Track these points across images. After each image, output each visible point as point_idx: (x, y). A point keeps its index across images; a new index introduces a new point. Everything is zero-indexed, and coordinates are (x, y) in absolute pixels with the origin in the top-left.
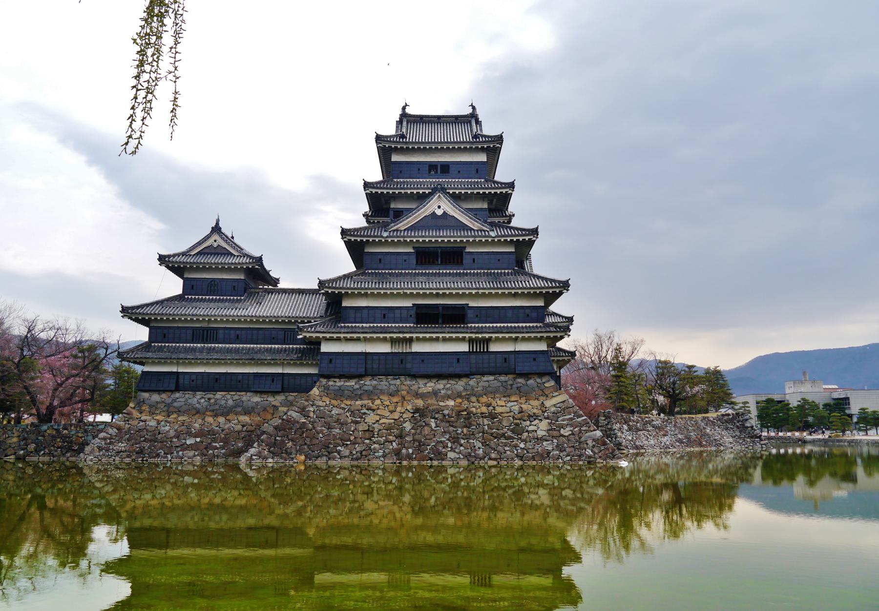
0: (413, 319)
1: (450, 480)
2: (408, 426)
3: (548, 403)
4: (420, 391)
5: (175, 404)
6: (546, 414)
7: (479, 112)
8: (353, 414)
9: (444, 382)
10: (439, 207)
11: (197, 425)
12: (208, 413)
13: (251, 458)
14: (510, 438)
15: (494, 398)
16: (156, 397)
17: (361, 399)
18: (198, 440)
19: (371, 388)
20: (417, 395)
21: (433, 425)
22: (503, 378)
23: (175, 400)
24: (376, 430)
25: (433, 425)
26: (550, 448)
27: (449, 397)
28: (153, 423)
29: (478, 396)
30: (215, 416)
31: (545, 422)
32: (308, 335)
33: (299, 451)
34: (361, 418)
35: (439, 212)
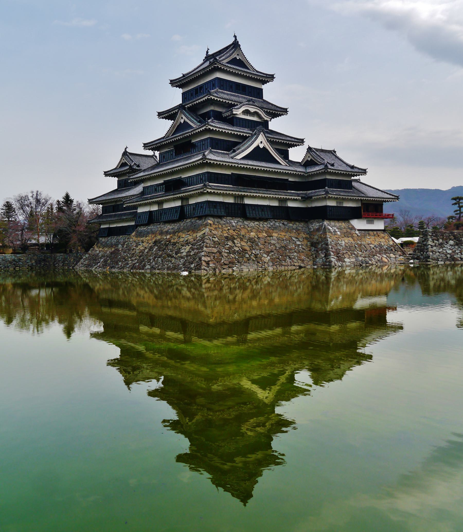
0: (164, 190)
2: (146, 251)
5: (108, 243)
7: (238, 39)
9: (173, 224)
11: (108, 252)
13: (96, 268)
14: (173, 257)
16: (103, 240)
19: (149, 230)
20: (161, 233)
21: (154, 250)
22: (193, 220)
23: (108, 241)
25: (154, 250)
27: (170, 234)
28: (98, 252)
29: (179, 232)
32: (127, 205)
33: (109, 265)
35: (182, 121)
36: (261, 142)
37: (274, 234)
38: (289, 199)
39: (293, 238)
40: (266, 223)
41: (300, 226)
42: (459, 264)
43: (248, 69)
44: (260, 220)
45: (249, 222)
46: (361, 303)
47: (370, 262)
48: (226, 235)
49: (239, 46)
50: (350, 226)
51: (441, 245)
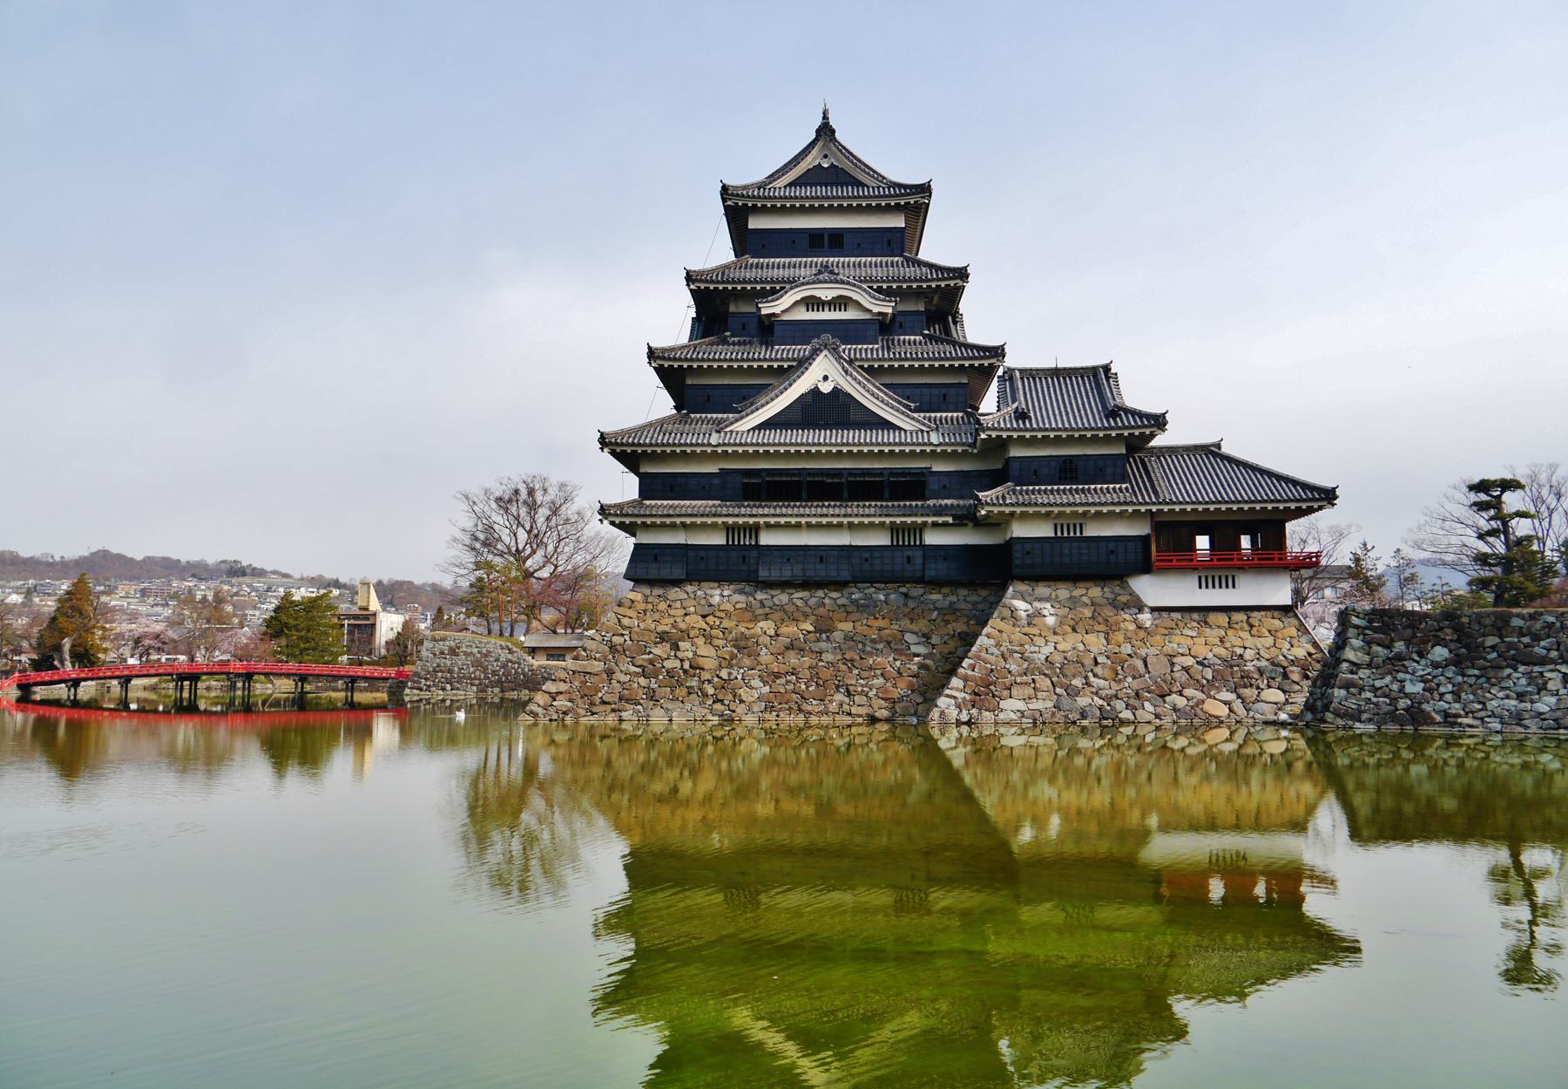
36: (826, 378)
37: (841, 626)
38: (925, 524)
39: (909, 637)
40: (834, 595)
41: (974, 598)
42: (1434, 738)
43: (860, 184)
44: (806, 585)
45: (774, 592)
46: (1165, 849)
47: (1127, 715)
48: (667, 628)
49: (833, 131)
50: (1124, 599)
51: (1396, 663)
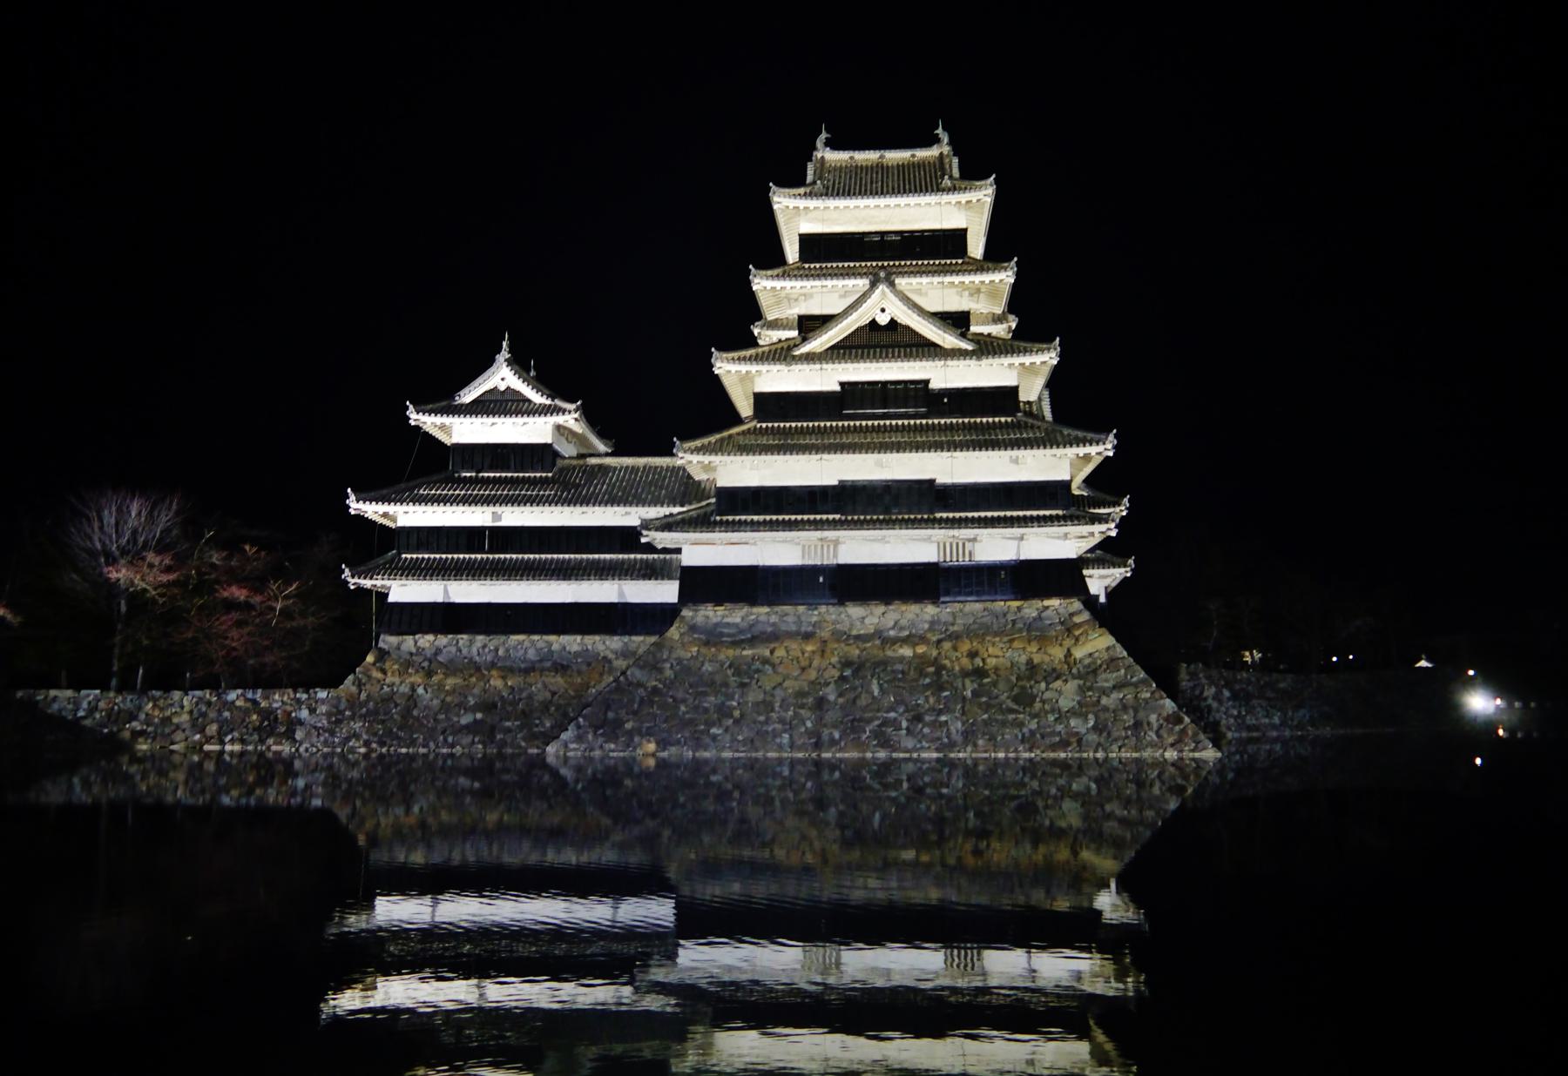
1: (905, 785)
3: (1079, 653)
4: (854, 632)
6: (1074, 671)
8: (738, 673)
10: (883, 310)
12: (494, 673)
14: (1011, 711)
15: (982, 642)
17: (752, 646)
18: (479, 716)
24: (778, 699)
26: (1083, 731)
27: (905, 641)
28: (404, 689)
30: (504, 678)
31: (1072, 686)
34: (752, 678)
35: (883, 320)
